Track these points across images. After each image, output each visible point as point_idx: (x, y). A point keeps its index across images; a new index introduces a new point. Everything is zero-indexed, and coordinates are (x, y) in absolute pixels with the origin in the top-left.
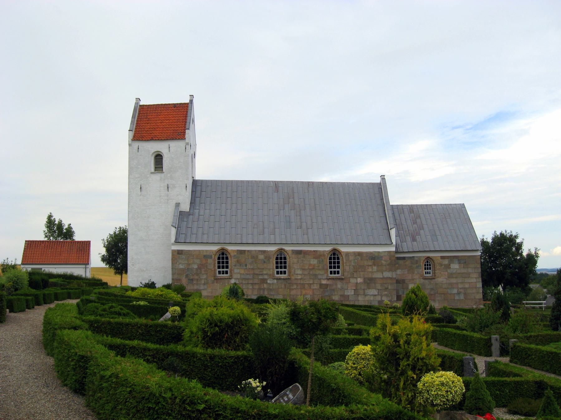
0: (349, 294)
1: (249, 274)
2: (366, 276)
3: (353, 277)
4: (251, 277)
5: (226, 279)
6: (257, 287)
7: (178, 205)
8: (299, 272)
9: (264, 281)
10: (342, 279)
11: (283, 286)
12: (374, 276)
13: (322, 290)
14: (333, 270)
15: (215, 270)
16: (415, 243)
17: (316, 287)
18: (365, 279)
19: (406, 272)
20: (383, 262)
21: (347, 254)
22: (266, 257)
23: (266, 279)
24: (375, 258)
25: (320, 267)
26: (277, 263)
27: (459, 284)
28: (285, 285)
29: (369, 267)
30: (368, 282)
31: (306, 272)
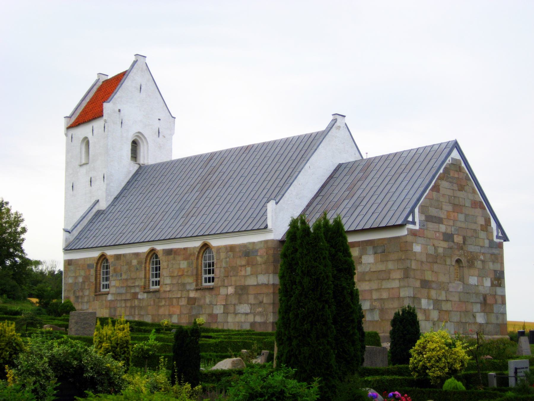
2: (238, 284)
3: (224, 286)
6: (129, 304)
11: (152, 303)
12: (247, 284)
13: (189, 306)
17: (183, 302)
18: (236, 287)
21: (219, 249)
24: (249, 252)
29: (243, 268)
30: (240, 292)
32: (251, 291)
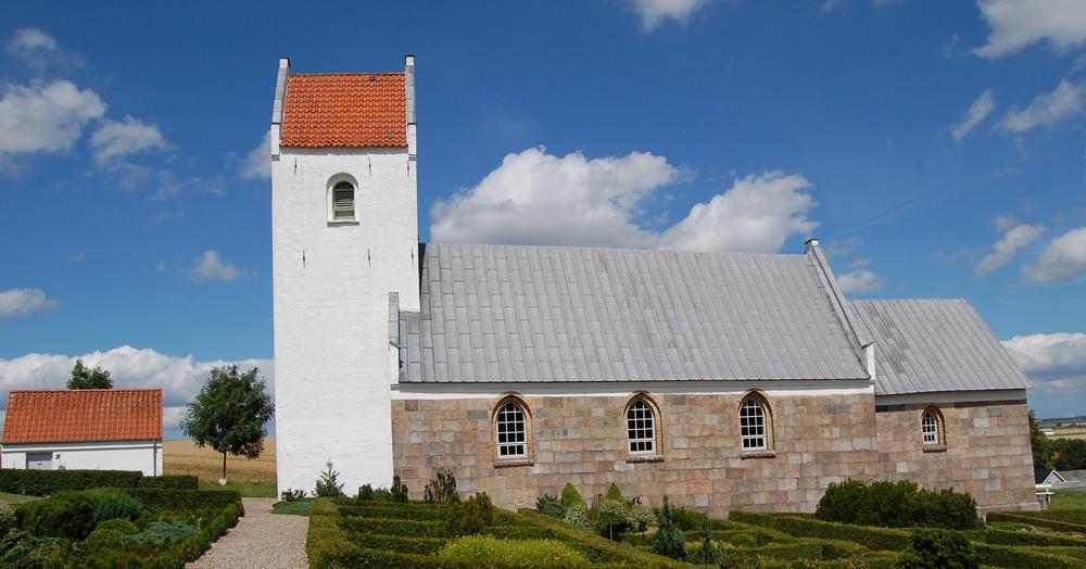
0: (786, 488)
1: (575, 452)
2: (820, 449)
4: (578, 458)
5: (520, 465)
7: (394, 298)
8: (682, 443)
9: (606, 467)
10: (773, 457)
11: (648, 477)
12: (834, 449)
13: (731, 482)
14: (749, 437)
15: (494, 446)
16: (903, 376)
17: (717, 475)
18: (817, 454)
19: (891, 438)
20: (851, 417)
21: (780, 401)
22: (608, 413)
23: (612, 463)
25: (725, 433)
26: (631, 425)
27: (992, 460)
28: (653, 474)
29: (826, 430)
31: (695, 444)
32: (845, 459)
